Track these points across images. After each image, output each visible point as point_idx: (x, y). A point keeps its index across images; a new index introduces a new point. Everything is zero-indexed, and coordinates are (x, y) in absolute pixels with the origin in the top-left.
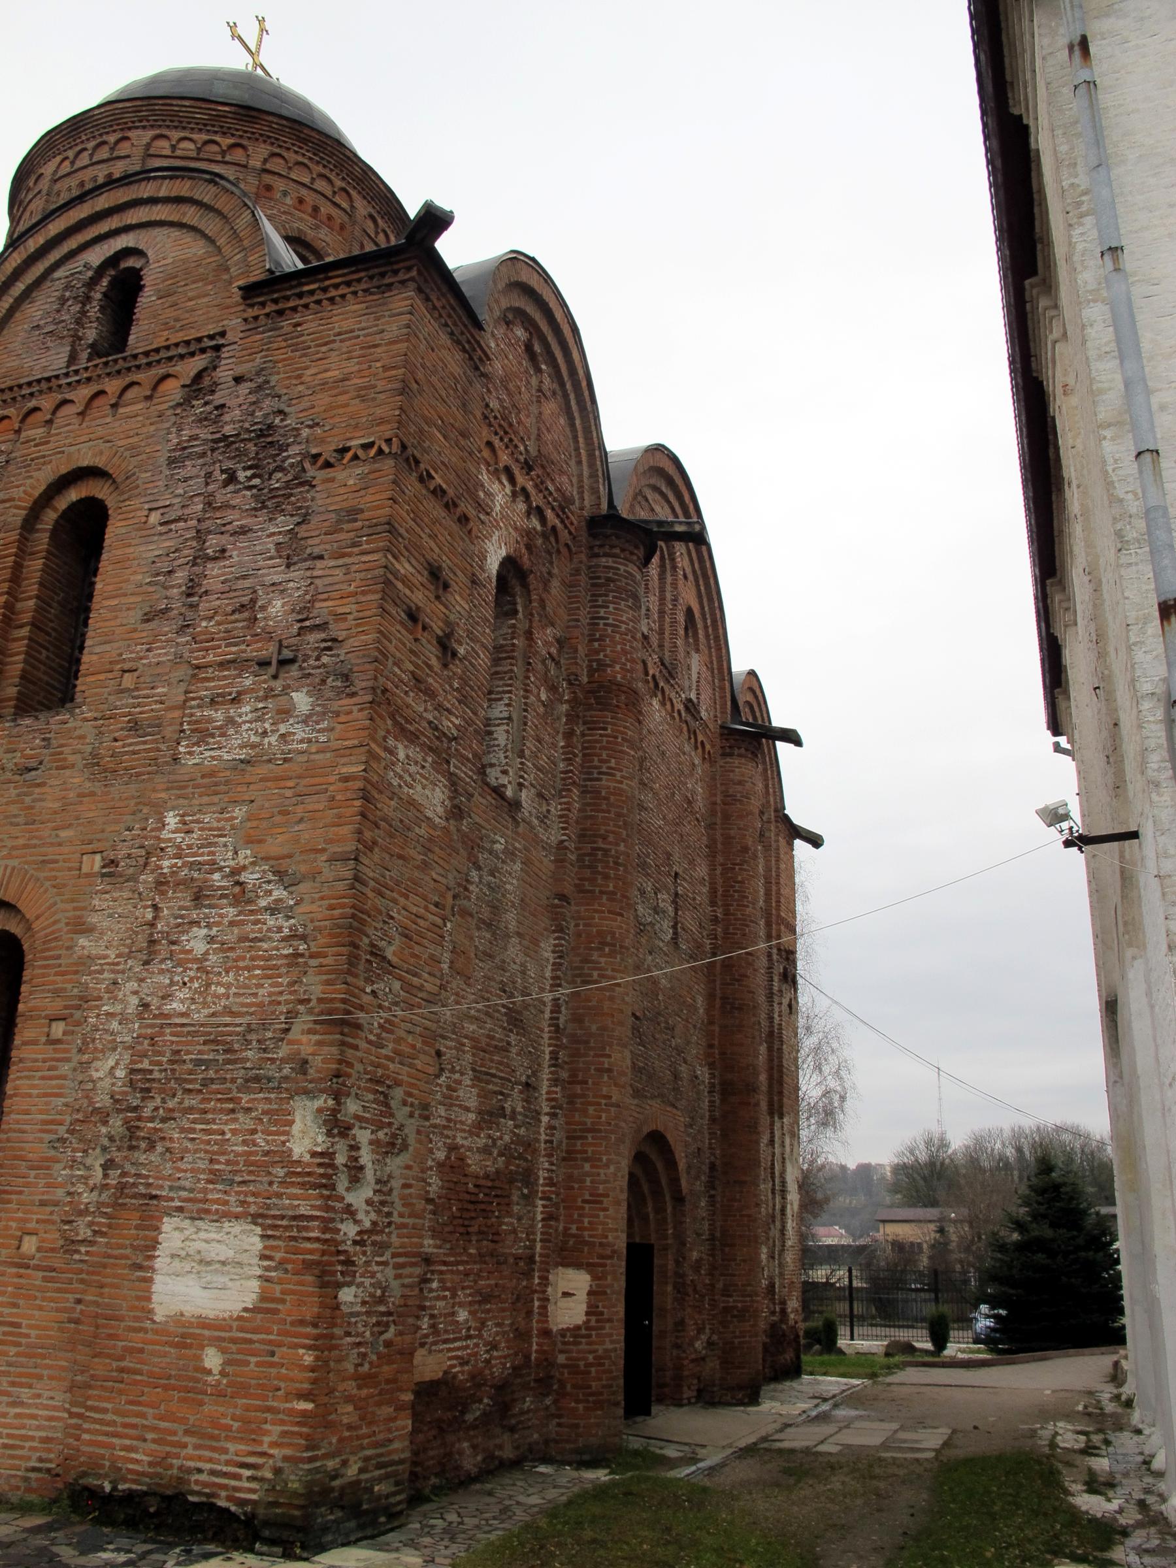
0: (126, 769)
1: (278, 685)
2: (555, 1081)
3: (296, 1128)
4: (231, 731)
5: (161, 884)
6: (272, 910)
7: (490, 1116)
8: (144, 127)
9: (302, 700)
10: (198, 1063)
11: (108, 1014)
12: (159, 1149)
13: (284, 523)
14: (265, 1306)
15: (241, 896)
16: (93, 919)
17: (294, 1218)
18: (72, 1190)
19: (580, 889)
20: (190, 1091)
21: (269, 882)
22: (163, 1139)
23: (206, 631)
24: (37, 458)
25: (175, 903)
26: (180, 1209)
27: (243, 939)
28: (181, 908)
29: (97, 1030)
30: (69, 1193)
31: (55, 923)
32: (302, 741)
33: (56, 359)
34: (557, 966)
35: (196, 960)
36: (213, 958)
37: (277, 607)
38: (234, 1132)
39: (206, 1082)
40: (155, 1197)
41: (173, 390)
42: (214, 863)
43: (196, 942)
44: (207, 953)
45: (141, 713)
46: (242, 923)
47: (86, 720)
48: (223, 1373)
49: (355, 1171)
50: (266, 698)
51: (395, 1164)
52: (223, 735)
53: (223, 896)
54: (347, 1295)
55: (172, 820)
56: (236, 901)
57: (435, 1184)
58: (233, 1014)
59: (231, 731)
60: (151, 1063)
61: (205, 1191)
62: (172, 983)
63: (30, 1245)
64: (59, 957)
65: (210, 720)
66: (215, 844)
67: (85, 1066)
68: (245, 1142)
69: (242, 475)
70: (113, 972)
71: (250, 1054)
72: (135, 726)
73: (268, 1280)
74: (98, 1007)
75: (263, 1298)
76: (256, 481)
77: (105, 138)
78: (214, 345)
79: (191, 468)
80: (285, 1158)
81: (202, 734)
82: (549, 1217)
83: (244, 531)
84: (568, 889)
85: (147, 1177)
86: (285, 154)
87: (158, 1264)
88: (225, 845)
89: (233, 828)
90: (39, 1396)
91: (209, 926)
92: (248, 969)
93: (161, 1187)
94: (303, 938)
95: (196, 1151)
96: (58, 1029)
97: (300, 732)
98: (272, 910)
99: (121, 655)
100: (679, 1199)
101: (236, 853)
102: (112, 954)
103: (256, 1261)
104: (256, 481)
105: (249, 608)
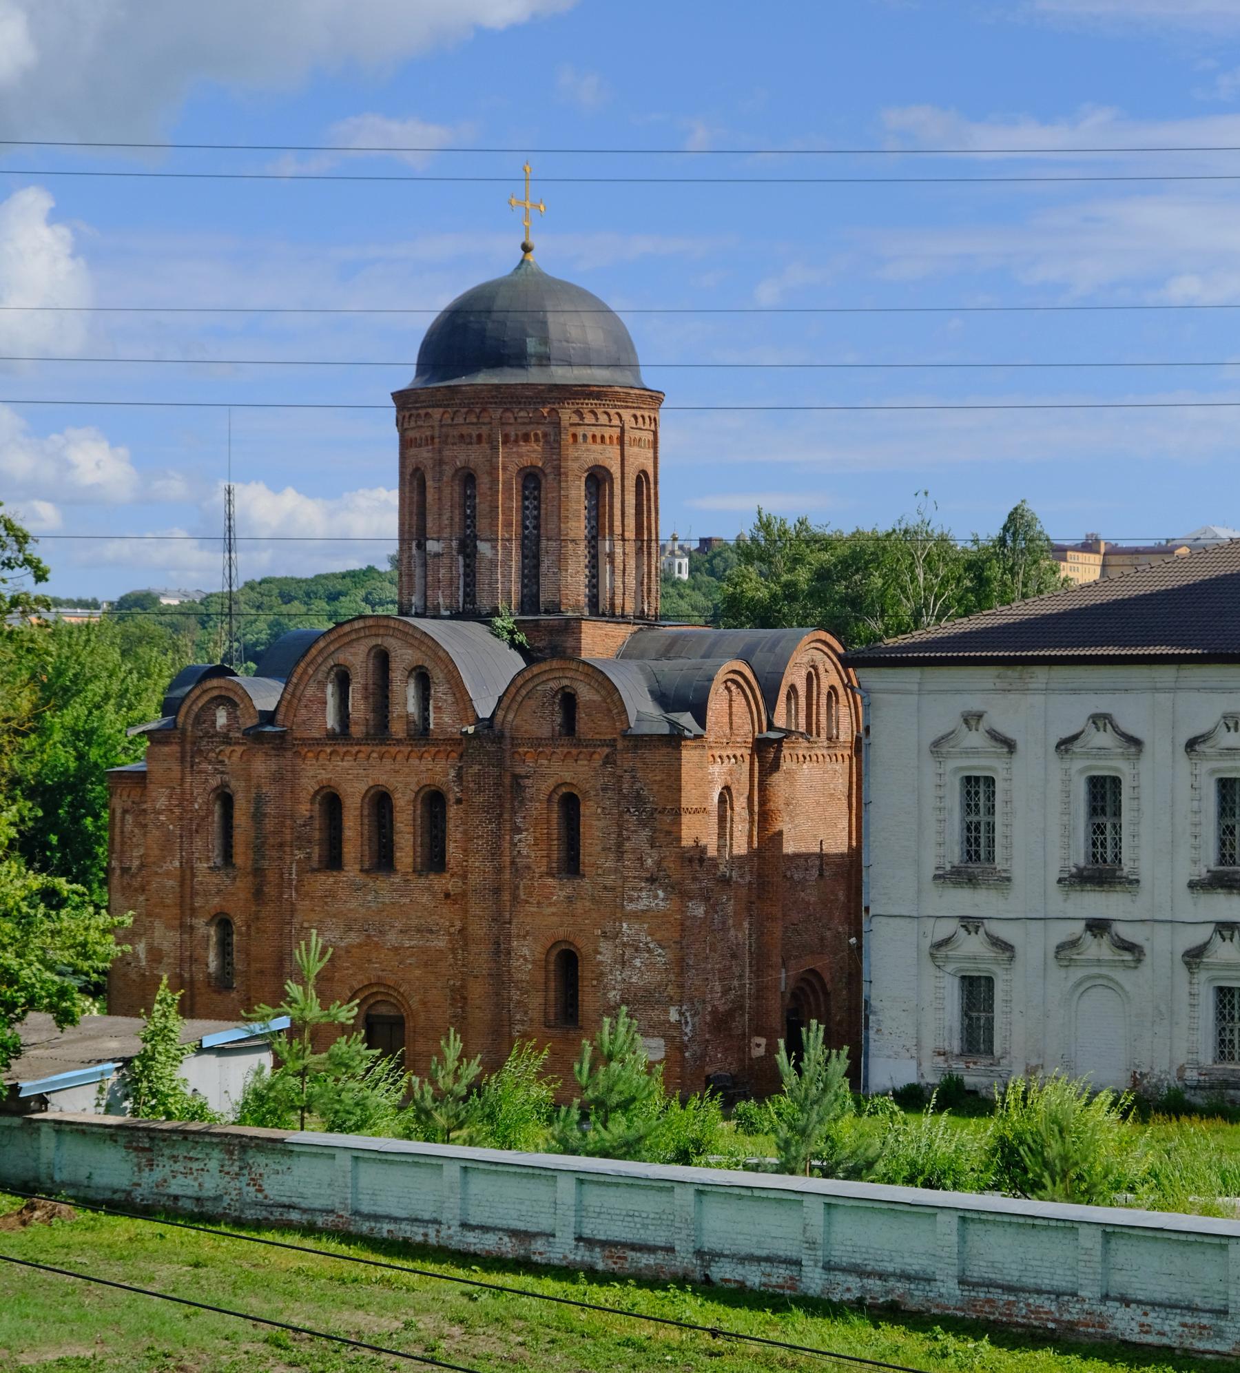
2: (751, 972)
5: (624, 945)
7: (726, 992)
9: (661, 894)
13: (646, 833)
15: (649, 951)
19: (759, 898)
25: (629, 952)
33: (545, 731)
37: (649, 861)
41: (597, 761)
43: (637, 962)
49: (687, 1023)
51: (696, 1019)
54: (687, 1054)
55: (625, 925)
57: (708, 1018)
67: (605, 994)
72: (605, 888)
78: (612, 744)
79: (610, 794)
80: (669, 1022)
81: (631, 900)
82: (750, 1020)
83: (635, 831)
84: (753, 899)
96: (595, 983)
97: (661, 903)
100: (826, 994)
105: (641, 860)
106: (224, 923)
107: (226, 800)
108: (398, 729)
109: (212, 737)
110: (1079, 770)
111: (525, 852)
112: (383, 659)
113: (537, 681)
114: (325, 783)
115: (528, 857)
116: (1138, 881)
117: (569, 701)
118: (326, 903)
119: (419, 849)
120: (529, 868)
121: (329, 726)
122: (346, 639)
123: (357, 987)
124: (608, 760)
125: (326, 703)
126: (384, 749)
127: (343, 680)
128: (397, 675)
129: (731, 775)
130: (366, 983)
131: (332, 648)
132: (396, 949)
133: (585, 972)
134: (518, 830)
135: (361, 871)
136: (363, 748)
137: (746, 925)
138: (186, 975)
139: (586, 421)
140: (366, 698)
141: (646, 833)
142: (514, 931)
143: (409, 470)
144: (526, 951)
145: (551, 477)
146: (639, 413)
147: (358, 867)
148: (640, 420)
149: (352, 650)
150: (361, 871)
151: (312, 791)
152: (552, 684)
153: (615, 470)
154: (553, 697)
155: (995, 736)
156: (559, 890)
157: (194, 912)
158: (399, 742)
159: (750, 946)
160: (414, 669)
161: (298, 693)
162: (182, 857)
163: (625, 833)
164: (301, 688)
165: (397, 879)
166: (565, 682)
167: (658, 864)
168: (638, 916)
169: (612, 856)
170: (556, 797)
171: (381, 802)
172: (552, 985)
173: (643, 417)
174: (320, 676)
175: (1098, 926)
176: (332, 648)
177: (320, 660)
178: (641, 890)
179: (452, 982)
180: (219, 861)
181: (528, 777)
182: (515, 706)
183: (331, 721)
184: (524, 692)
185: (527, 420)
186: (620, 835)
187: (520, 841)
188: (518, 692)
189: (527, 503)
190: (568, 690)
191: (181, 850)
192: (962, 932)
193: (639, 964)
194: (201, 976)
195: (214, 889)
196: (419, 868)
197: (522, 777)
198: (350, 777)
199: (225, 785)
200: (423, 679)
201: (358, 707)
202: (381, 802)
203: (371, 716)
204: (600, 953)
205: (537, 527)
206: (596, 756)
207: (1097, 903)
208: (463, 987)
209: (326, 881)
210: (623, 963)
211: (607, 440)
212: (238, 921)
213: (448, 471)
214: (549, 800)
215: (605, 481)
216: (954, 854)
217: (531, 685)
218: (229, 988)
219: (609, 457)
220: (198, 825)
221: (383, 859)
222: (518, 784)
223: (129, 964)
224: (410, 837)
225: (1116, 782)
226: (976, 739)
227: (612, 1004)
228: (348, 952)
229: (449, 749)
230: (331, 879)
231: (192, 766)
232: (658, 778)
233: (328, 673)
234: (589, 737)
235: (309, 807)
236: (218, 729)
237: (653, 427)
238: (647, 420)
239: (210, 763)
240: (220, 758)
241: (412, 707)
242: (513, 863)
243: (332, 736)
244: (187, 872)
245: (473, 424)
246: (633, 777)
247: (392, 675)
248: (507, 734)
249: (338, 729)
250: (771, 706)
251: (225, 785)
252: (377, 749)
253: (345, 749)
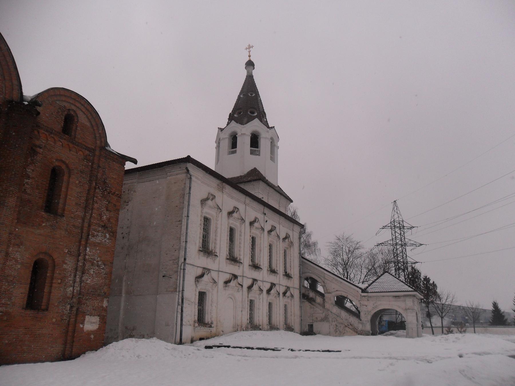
0: (73, 234)
3: (104, 303)
4: (98, 237)
6: (103, 269)
10: (92, 291)
11: (69, 280)
12: (86, 305)
14: (99, 328)
15: (98, 266)
16: (66, 262)
17: (103, 316)
18: (63, 311)
20: (90, 296)
21: (102, 264)
22: (86, 303)
23: (94, 216)
24: (53, 151)
26: (88, 314)
27: (99, 272)
28: (89, 265)
29: (68, 283)
30: (62, 311)
31: (59, 261)
32: (107, 243)
35: (92, 275)
36: (94, 275)
37: (105, 217)
38: (96, 303)
39: (93, 295)
40: (85, 312)
42: (94, 259)
44: (93, 274)
45: (75, 224)
46: (98, 270)
47: (65, 221)
48: (93, 338)
50: (103, 233)
52: (96, 237)
53: (96, 265)
55: (88, 249)
56: (97, 267)
58: (96, 284)
59: (98, 237)
60: (84, 291)
61: (92, 311)
62: (88, 278)
63: (54, 320)
64: (60, 267)
65: (94, 233)
66: (95, 256)
67: (65, 289)
68: (98, 305)
69: (101, 188)
70: (70, 272)
71: (99, 291)
72: (74, 226)
73: (100, 324)
74: (68, 278)
75: (99, 327)
76: (101, 190)
85: (83, 309)
87: (85, 323)
88: (96, 256)
89: (97, 253)
90: (57, 346)
91: (93, 269)
92: (99, 278)
93: (86, 311)
94: (107, 274)
95: (91, 305)
97: (107, 241)
98: (103, 269)
99: (71, 210)
101: (97, 258)
102: (70, 269)
103: (98, 322)
104: (101, 190)
105: (101, 216)
111: (28, 191)
144: (18, 256)
152: (66, 104)
166: (73, 107)
167: (109, 220)
168: (95, 245)
178: (98, 232)
181: (41, 148)
187: (27, 183)
193: (92, 273)
204: (66, 263)
227: (68, 295)
246: (104, 172)
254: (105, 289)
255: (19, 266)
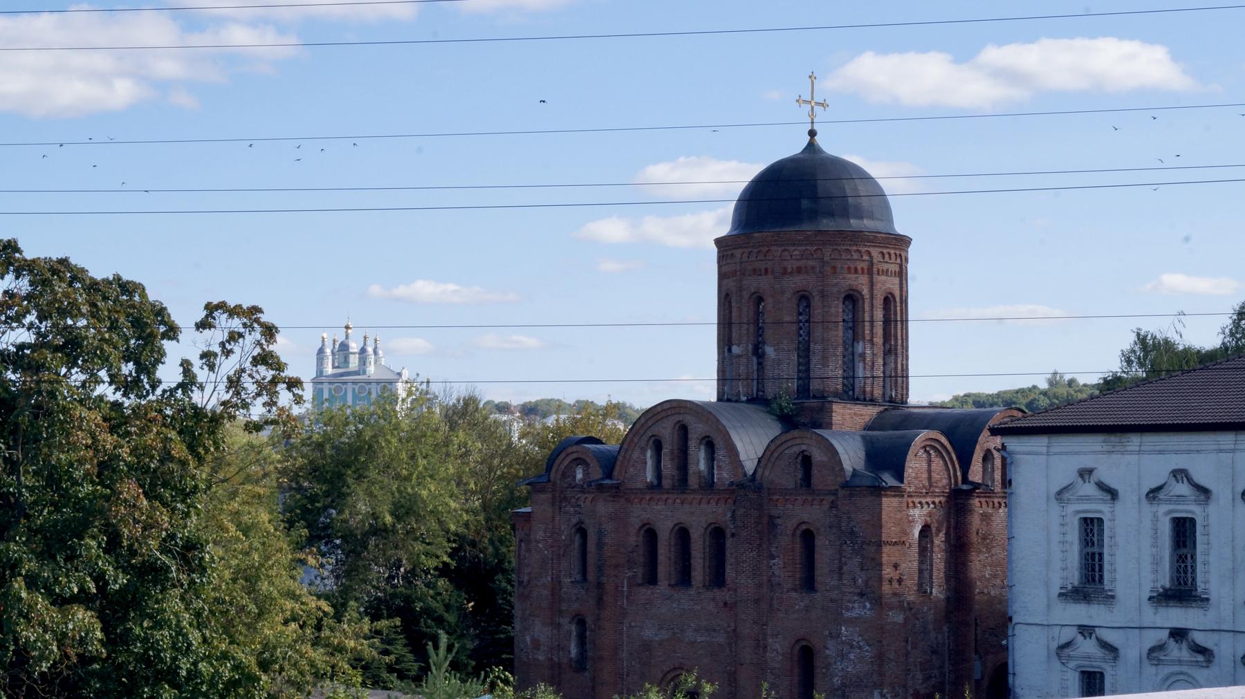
1: (862, 600)
5: (843, 642)
6: (867, 651)
8: (777, 245)
9: (868, 605)
13: (857, 560)
15: (860, 648)
16: (828, 646)
34: (949, 632)
41: (826, 506)
55: (843, 629)
69: (848, 542)
77: (761, 248)
78: (835, 493)
81: (848, 609)
86: (839, 248)
96: (824, 670)
97: (868, 612)
98: (867, 651)
105: (854, 580)
106: (581, 623)
107: (582, 532)
108: (693, 481)
109: (573, 488)
110: (1163, 516)
111: (777, 573)
112: (684, 430)
113: (785, 446)
114: (645, 522)
115: (779, 577)
116: (1207, 599)
117: (806, 461)
118: (646, 608)
119: (707, 570)
120: (779, 584)
121: (648, 480)
122: (659, 417)
123: (667, 669)
124: (833, 505)
125: (646, 463)
126: (684, 496)
127: (658, 446)
128: (692, 444)
129: (930, 516)
130: (672, 667)
131: (650, 423)
132: (692, 643)
133: (818, 663)
134: (773, 557)
135: (669, 585)
136: (671, 496)
137: (945, 629)
138: (556, 659)
139: (843, 257)
140: (672, 459)
141: (857, 560)
142: (769, 632)
143: (724, 294)
144: (778, 646)
145: (817, 298)
146: (885, 251)
147: (667, 583)
148: (887, 256)
149: (663, 425)
150: (669, 585)
151: (637, 527)
153: (865, 292)
154: (796, 458)
155: (1102, 486)
156: (799, 601)
157: (561, 613)
158: (694, 491)
159: (949, 645)
160: (703, 438)
161: (628, 457)
162: (553, 574)
163: (843, 559)
164: (630, 452)
165: (692, 592)
166: (804, 447)
167: (866, 582)
168: (851, 622)
169: (836, 577)
170: (799, 532)
171: (683, 535)
172: (796, 671)
173: (889, 254)
174: (643, 443)
175: (1178, 634)
176: (650, 423)
177: (642, 432)
179: (728, 668)
180: (579, 577)
181: (779, 517)
182: (770, 465)
183: (650, 476)
184: (776, 455)
185: (798, 257)
186: (840, 561)
187: (774, 564)
188: (772, 454)
189: (801, 318)
190: (806, 453)
191: (553, 568)
192: (1080, 638)
193: (852, 658)
194: (566, 661)
195: (574, 598)
196: (707, 584)
197: (775, 518)
198: (662, 517)
199: (581, 522)
200: (710, 446)
201: (668, 466)
202: (683, 535)
203: (675, 472)
205: (809, 334)
206: (824, 502)
207: (1177, 616)
208: (735, 672)
209: (645, 593)
210: (843, 657)
211: (860, 271)
212: (589, 621)
213: (746, 295)
214: (794, 534)
215: (858, 300)
216: (1074, 577)
217: (780, 449)
218: (584, 669)
219: (862, 282)
220: (565, 551)
221: (684, 578)
222: (773, 523)
223: (522, 650)
224: (701, 561)
225: (1193, 521)
226: (1089, 489)
228: (660, 644)
229: (727, 496)
230: (649, 591)
231: (560, 508)
232: (866, 519)
233: (648, 441)
234: (819, 488)
235: (635, 538)
236: (577, 481)
237: (899, 261)
238: (893, 256)
239: (572, 506)
240: (578, 503)
241: (702, 466)
242: (769, 581)
243: (651, 487)
244: (556, 585)
245: (761, 260)
246: (849, 518)
247: (690, 443)
248: (765, 486)
249: (655, 482)
250: (965, 463)
251: (581, 522)
252: (680, 496)
253: (658, 497)
254: (875, 678)
255: (780, 658)
